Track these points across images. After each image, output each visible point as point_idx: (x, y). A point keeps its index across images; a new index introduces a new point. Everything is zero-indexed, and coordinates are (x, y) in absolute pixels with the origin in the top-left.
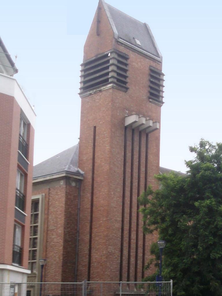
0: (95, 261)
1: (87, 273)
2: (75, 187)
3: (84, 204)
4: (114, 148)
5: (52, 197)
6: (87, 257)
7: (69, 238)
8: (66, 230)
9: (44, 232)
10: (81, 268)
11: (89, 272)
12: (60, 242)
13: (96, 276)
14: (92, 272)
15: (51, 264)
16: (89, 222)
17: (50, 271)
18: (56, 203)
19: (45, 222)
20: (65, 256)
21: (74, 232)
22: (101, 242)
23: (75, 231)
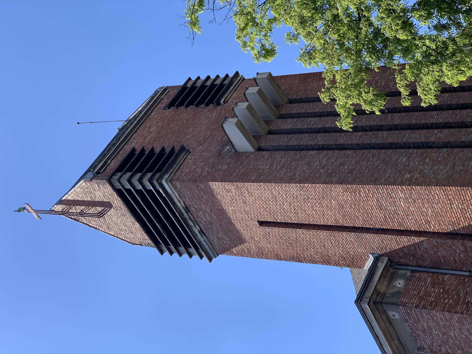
2: (408, 280)
3: (455, 260)
4: (294, 175)
5: (440, 346)
18: (455, 335)
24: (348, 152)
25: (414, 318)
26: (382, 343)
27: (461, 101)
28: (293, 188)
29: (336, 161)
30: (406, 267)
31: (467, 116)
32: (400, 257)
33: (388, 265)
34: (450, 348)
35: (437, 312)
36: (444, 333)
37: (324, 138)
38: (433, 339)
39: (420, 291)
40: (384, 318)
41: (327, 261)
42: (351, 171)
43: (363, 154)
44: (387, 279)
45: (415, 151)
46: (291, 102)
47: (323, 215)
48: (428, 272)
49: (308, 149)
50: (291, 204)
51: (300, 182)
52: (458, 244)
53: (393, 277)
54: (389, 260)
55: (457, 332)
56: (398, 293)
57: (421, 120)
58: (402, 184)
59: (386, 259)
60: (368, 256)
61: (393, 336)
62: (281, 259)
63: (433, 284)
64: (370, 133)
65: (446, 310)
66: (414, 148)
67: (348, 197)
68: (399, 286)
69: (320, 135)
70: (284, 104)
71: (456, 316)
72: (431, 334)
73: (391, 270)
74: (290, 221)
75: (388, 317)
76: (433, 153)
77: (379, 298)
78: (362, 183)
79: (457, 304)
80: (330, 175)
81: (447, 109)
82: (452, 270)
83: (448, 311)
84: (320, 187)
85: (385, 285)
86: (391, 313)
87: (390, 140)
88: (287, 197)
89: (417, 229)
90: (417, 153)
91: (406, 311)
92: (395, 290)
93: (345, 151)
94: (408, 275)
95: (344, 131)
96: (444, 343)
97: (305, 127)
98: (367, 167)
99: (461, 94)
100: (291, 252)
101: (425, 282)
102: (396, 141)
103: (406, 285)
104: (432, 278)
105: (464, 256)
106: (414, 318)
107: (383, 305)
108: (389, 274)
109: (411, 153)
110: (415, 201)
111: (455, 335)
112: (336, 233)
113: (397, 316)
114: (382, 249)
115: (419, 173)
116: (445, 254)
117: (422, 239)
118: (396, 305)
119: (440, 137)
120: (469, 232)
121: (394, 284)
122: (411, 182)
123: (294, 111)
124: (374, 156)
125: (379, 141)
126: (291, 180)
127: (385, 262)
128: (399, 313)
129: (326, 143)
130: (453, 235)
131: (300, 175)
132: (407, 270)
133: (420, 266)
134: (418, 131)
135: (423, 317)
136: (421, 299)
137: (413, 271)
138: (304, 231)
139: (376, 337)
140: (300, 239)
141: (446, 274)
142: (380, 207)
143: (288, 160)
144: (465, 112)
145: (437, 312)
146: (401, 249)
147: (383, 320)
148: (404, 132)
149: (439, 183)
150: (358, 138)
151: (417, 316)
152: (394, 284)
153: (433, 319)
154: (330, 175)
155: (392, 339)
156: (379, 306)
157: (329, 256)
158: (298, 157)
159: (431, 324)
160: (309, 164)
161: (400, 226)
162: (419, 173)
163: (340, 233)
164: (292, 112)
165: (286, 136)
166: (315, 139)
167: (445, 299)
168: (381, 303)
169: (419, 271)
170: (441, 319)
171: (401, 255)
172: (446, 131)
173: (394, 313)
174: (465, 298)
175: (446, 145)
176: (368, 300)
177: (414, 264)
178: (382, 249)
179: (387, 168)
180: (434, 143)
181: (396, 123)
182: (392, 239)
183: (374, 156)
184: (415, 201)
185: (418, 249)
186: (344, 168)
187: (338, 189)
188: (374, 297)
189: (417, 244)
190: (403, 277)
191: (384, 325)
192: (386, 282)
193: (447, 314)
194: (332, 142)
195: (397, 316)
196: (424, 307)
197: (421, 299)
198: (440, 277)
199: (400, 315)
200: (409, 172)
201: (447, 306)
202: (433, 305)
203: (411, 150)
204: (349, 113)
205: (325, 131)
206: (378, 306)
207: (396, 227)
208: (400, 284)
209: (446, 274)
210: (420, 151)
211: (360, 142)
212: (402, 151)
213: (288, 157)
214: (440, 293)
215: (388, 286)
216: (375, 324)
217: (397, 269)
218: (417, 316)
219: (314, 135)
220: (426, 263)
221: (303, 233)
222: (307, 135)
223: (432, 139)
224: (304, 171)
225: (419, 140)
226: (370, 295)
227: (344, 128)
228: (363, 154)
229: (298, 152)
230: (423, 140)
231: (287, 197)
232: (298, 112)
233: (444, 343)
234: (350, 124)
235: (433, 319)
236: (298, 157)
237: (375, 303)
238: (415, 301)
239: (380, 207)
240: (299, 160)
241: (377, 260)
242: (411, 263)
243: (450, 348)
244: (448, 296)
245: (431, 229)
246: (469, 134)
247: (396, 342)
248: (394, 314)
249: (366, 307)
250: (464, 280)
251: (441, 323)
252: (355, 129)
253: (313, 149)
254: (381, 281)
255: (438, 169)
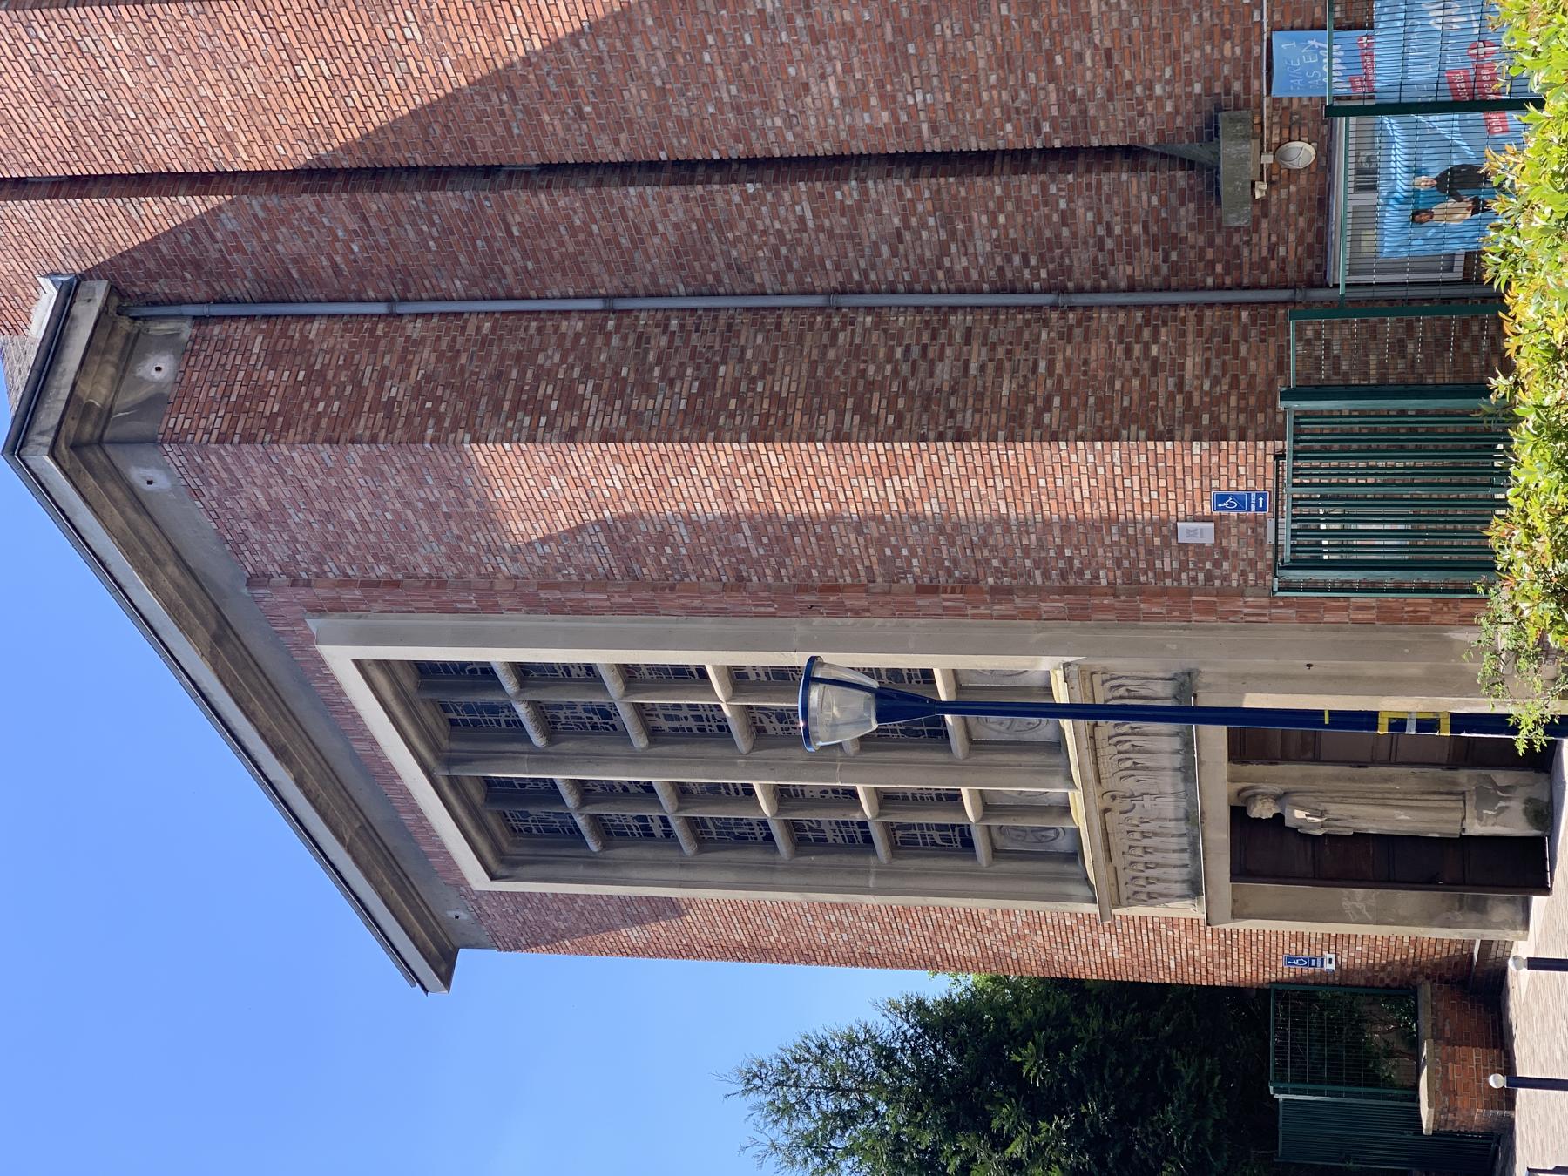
0: (887, 100)
1: (1028, 186)
2: (186, 353)
3: (334, 265)
5: (319, 560)
6: (849, 192)
7: (671, 383)
8: (595, 424)
9: (651, 609)
10: (981, 246)
11: (1021, 159)
12: (712, 469)
13: (1052, 78)
14: (1008, 136)
15: (952, 544)
16: (488, 200)
17: (1026, 551)
18: (360, 516)
19: (556, 609)
20: (851, 421)
21: (615, 341)
22: (670, 56)
23: (608, 336)
25: (220, 481)
26: (121, 580)
35: (292, 446)
36: (327, 516)
38: (294, 540)
39: (229, 386)
40: (117, 493)
44: (113, 358)
52: (336, 208)
53: (132, 350)
54: (113, 290)
55: (365, 505)
56: (156, 403)
59: (100, 289)
60: (37, 286)
61: (158, 551)
63: (273, 357)
65: (321, 435)
68: (158, 376)
71: (356, 453)
72: (283, 525)
73: (125, 324)
75: (131, 490)
77: (88, 428)
79: (357, 413)
82: (330, 301)
83: (329, 441)
85: (105, 381)
86: (137, 475)
92: (141, 394)
94: (185, 336)
96: (328, 548)
101: (246, 352)
103: (182, 371)
104: (267, 335)
105: (363, 248)
107: (108, 448)
108: (118, 341)
110: (168, 63)
111: (360, 516)
113: (162, 482)
114: (80, 252)
116: (298, 246)
117: (214, 200)
118: (153, 441)
120: (366, 163)
127: (99, 298)
128: (165, 468)
132: (181, 317)
135: (248, 471)
136: (236, 410)
137: (199, 320)
139: (99, 562)
141: (312, 317)
142: (50, 95)
145: (292, 446)
146: (150, 247)
147: (113, 500)
151: (228, 470)
153: (282, 473)
156: (94, 456)
159: (280, 491)
161: (133, 159)
167: (315, 403)
168: (100, 442)
169: (221, 319)
171: (152, 265)
173: (151, 473)
174: (380, 388)
176: (48, 439)
177: (201, 295)
184: (168, 63)
189: (201, 220)
190: (169, 342)
192: (110, 370)
193: (325, 450)
195: (162, 482)
196: (249, 438)
197: (236, 410)
198: (295, 329)
199: (170, 476)
202: (279, 428)
208: (158, 369)
209: (312, 317)
214: (297, 385)
217: (146, 318)
218: (228, 470)
220: (244, 286)
226: (54, 420)
233: (328, 548)
235: (282, 473)
237: (75, 447)
239: (50, 95)
241: (69, 294)
244: (326, 389)
247: (172, 569)
249: (43, 462)
250: (373, 330)
251: (312, 484)
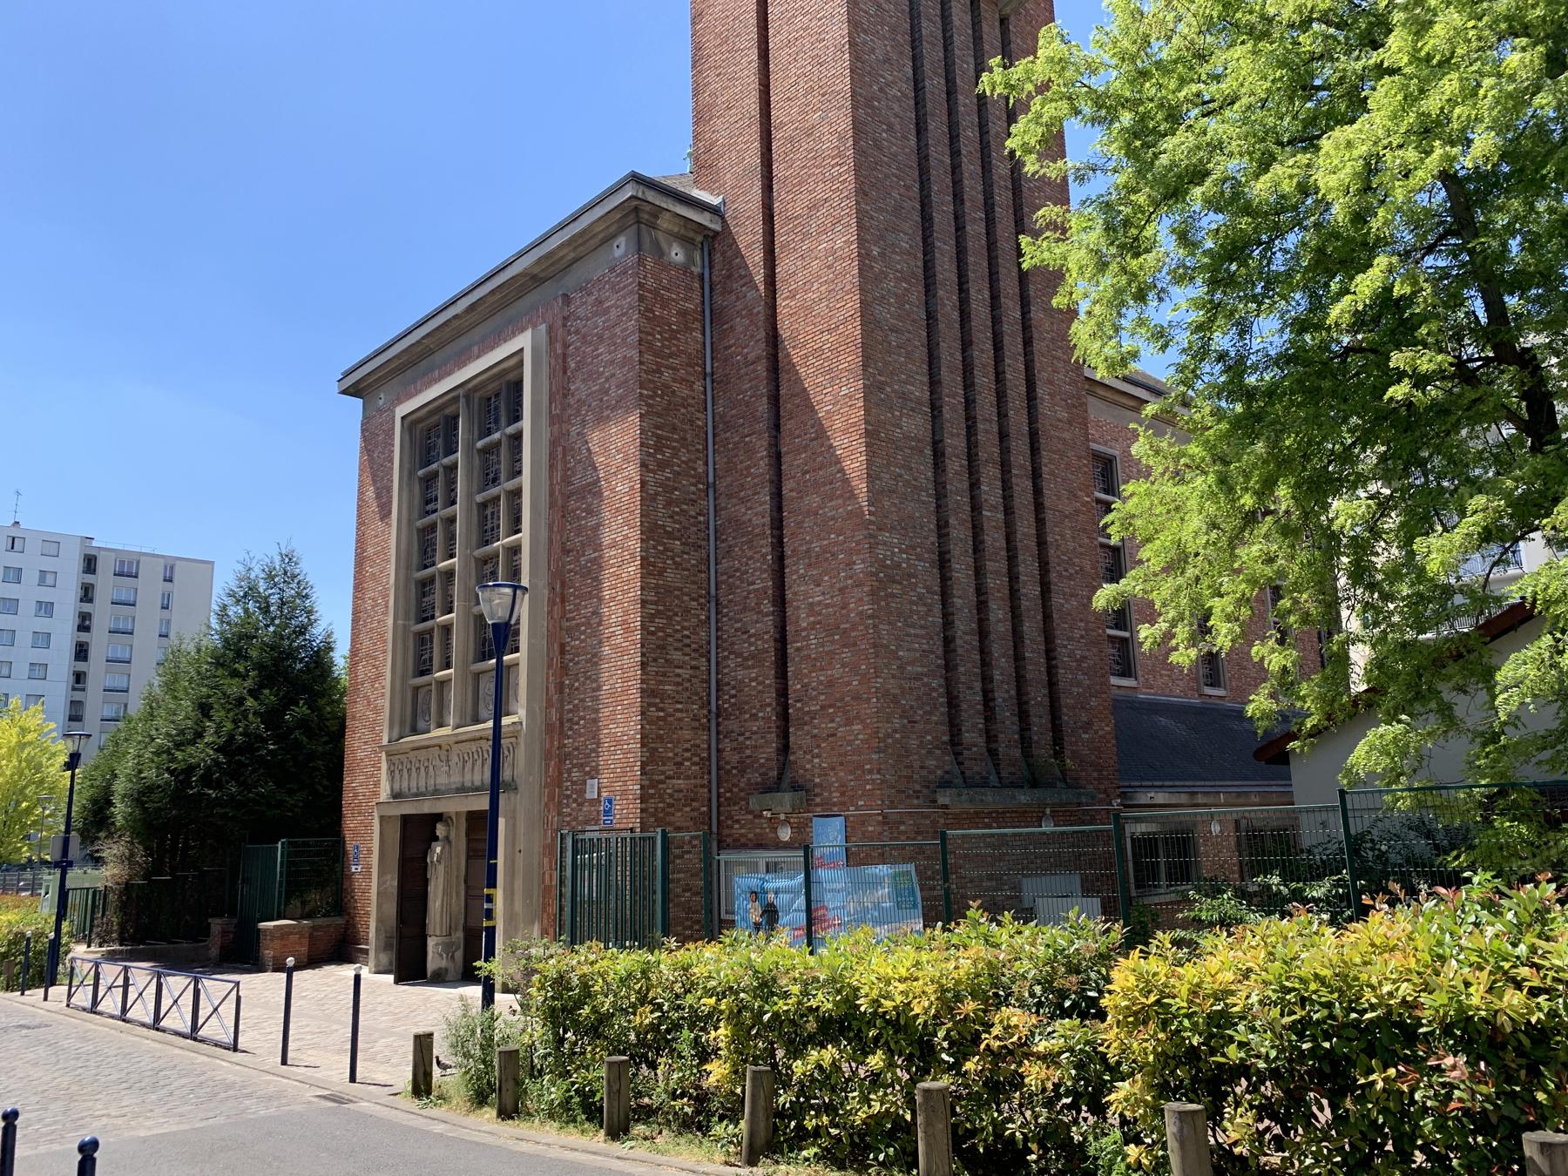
0: (812, 626)
1: (770, 697)
2: (685, 269)
3: (731, 347)
4: (865, 32)
5: (577, 332)
6: (767, 607)
7: (672, 517)
8: (650, 477)
9: (552, 505)
10: (740, 674)
11: (783, 693)
12: (626, 537)
13: (823, 708)
14: (795, 686)
15: (587, 661)
16: (762, 426)
17: (583, 700)
18: (601, 354)
19: (552, 456)
20: (651, 609)
21: (693, 488)
22: (833, 518)
23: (695, 485)
24: (913, 142)
25: (619, 282)
26: (566, 229)
27: (1007, 340)
28: (839, 31)
29: (896, 116)
30: (706, 263)
31: (982, 351)
32: (723, 253)
33: (706, 232)
34: (577, 349)
35: (637, 320)
36: (600, 337)
37: (937, 92)
38: (587, 320)
39: (668, 290)
40: (613, 229)
41: (701, 117)
42: (879, 148)
43: (911, 167)
44: (682, 231)
45: (920, 264)
46: (1004, 21)
47: (789, 99)
48: (703, 303)
49: (914, 59)
50: (805, 30)
51: (852, 44)
52: (758, 349)
53: (686, 241)
54: (717, 233)
55: (606, 357)
56: (660, 252)
57: (975, 271)
58: (861, 241)
59: (717, 227)
60: (718, 195)
61: (582, 248)
62: (694, 24)
63: (683, 313)
64: (948, 180)
65: (643, 336)
66: (925, 263)
67: (829, 143)
68: (673, 254)
69: (943, 81)
70: (1000, 6)
71: (634, 353)
72: (595, 314)
73: (699, 238)
74: (771, 32)
75: (614, 236)
76: (916, 295)
77: (646, 216)
78: (858, 168)
79: (656, 355)
80: (868, 103)
81: (993, 317)
82: (712, 344)
83: (641, 340)
84: (844, 85)
85: (670, 227)
86: (622, 240)
87: (937, 217)
88: (820, 19)
89: (778, 277)
90: (917, 266)
91: (632, 267)
92: (664, 245)
93: (914, 132)
94: (693, 268)
95: (978, 77)
96: (584, 337)
97: (957, 52)
98: (887, 176)
99: (1019, 340)
100: (710, 43)
101: (686, 300)
102: (936, 228)
103: (676, 266)
104: (695, 311)
105: (738, 362)
106: (619, 282)
107: (635, 226)
108: (691, 234)
109: (915, 257)
110: (829, 267)
111: (601, 354)
112: (756, 128)
113: (618, 253)
114: (735, 218)
115: (882, 272)
116: (739, 329)
117: (762, 288)
118: (639, 249)
119: (945, 305)
120: (781, 365)
121: (675, 245)
122: (864, 257)
123: (985, 28)
124: (907, 188)
125: (934, 198)
126: (854, 24)
127: (712, 226)
128: (626, 254)
129: (928, 96)
130: (774, 339)
131: (865, 43)
132: (703, 267)
133: (711, 290)
134: (954, 266)
135: (624, 297)
136: (656, 293)
137: (701, 277)
138: (755, 64)
139: (575, 218)
140: (738, 58)
141: (704, 334)
142: (814, 207)
143: (891, 17)
144: (989, 346)
145: (637, 320)
146: (738, 253)
147: (608, 227)
148: (953, 242)
149: (865, 306)
150: (965, 103)
151: (625, 287)
152: (675, 245)
153: (624, 315)
154: (868, 103)
155: (575, 248)
156: (631, 219)
157: (710, 119)
158: (899, 37)
159: (613, 313)
160: (887, 60)
161: (782, 247)
162: (882, 272)
163: (757, 136)
164: (984, 25)
165: (939, 12)
166: (935, 73)
167: (659, 333)
168: (638, 222)
169: (702, 288)
170: (626, 329)
171: (729, 254)
172: (956, 315)
173: (623, 246)
174: (667, 367)
175: (931, 317)
176: (640, 195)
177: (714, 278)
178: (735, 218)
179: (887, 212)
180: (935, 296)
181: (968, 228)
182: (754, 234)
183: (907, 188)
184: (829, 267)
185: (742, 282)
186: (884, 130)
187: (845, 124)
188: (648, 208)
189: (752, 280)
190: (690, 260)
191: (598, 230)
192: (676, 230)
193: (636, 337)
194: (929, 105)
195: (618, 253)
196: (641, 299)
197: (656, 293)
198: (697, 325)
199: (621, 257)
200: (882, 255)
201: (650, 338)
202: (647, 314)
203: (920, 255)
204: (1013, 87)
205: (977, 39)
206: (633, 216)
207: (779, 240)
208: (677, 254)
209: (704, 334)
210: (920, 271)
211: (933, 162)
212: (919, 239)
213: (898, 18)
214: (669, 325)
215: (668, 233)
216: (599, 212)
217: (702, 249)
218: (625, 287)
219: (941, 71)
220: (718, 299)
221: (750, 63)
222: (941, 55)
223: (941, 293)
224: (873, 51)
225: (938, 268)
226: (650, 199)
227: (985, 77)
228: (911, 167)
229: (908, 38)
230: (940, 277)
231: (820, 19)
232: (985, 36)
233: (584, 337)
234: (993, 89)
235: (624, 315)
236: (899, 37)
237: (636, 209)
238: (650, 282)
239: (814, 207)
240: (893, 40)
241: (714, 211)
242: (715, 272)
243: (577, 349)
244: (666, 339)
245: (781, 302)
246: (951, 355)
247: (572, 255)
248: (621, 247)
249: (628, 192)
250: (697, 365)
251: (618, 330)
252: (982, 98)
253: (915, 69)
254: (677, 220)
255: (890, 304)
